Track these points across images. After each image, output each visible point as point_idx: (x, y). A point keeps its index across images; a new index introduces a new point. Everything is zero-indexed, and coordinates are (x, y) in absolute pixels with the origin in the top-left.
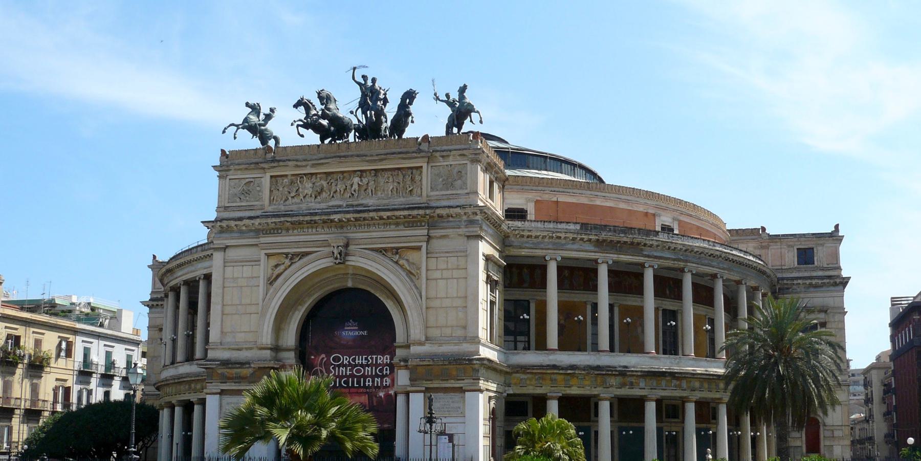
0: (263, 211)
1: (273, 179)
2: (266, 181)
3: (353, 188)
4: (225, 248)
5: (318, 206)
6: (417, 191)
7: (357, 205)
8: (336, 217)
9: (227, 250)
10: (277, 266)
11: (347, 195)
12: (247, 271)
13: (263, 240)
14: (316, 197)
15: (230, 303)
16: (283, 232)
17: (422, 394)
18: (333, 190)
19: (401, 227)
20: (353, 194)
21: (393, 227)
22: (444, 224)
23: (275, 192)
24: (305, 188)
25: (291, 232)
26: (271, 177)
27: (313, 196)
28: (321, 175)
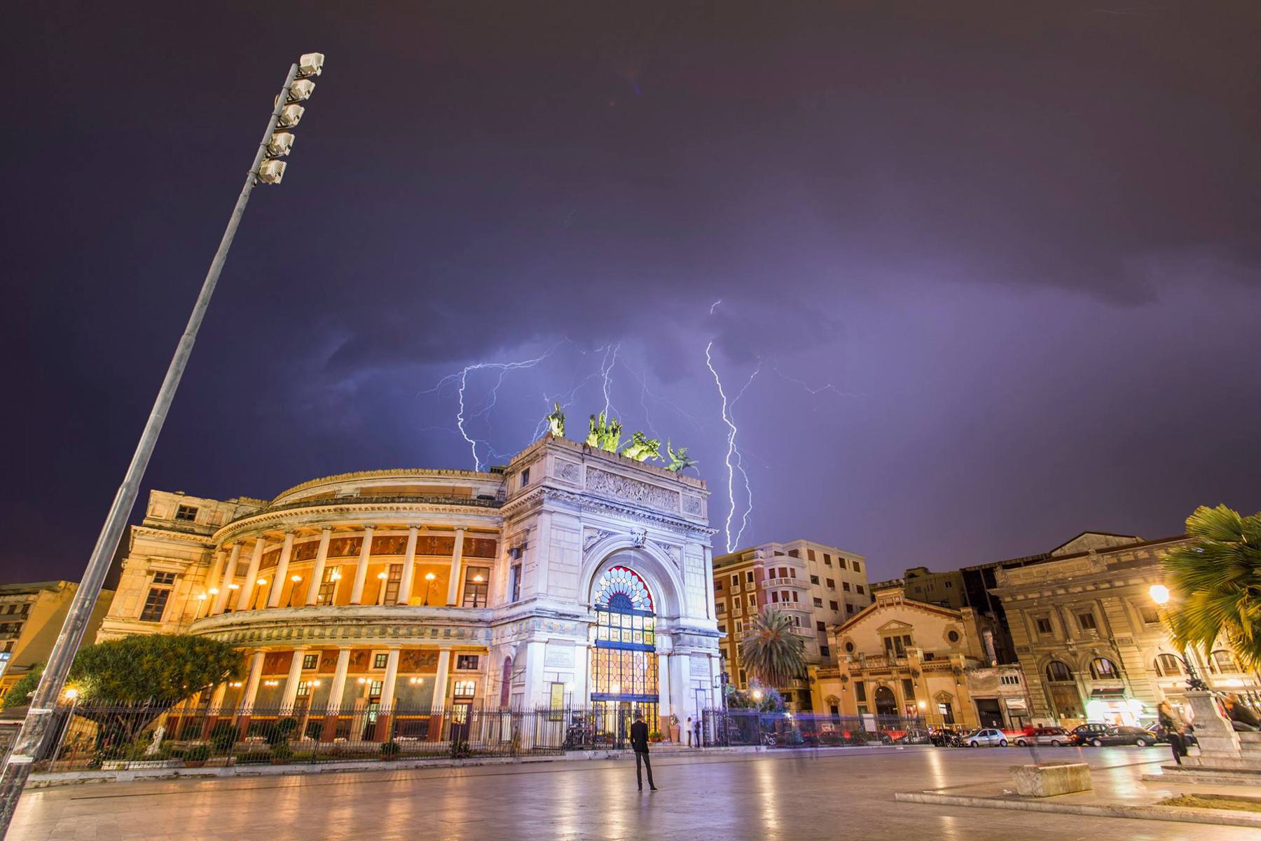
1: (589, 470)
2: (583, 468)
4: (553, 512)
6: (675, 508)
9: (553, 514)
10: (589, 538)
12: (568, 536)
13: (583, 514)
14: (616, 492)
15: (554, 561)
17: (688, 657)
19: (671, 530)
20: (640, 499)
21: (667, 529)
22: (693, 536)
23: (589, 479)
25: (603, 514)
27: (615, 491)
28: (620, 478)
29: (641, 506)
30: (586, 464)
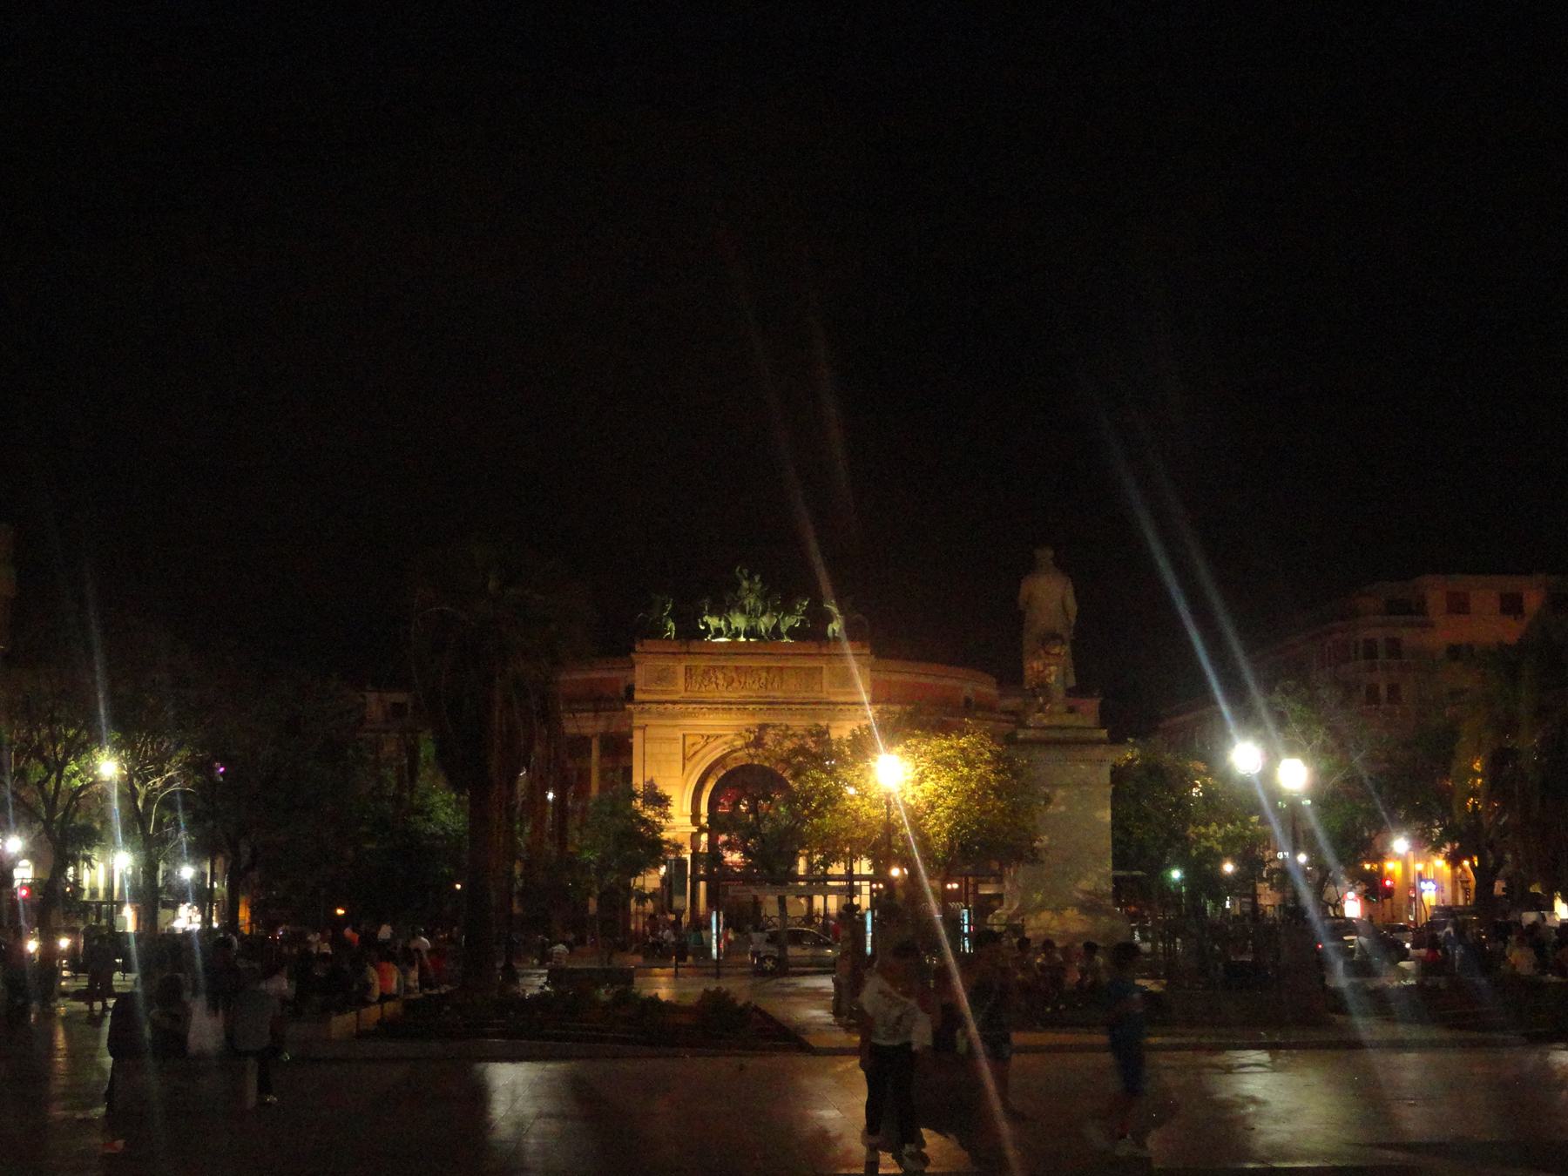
0: (680, 695)
2: (681, 669)
3: (762, 681)
5: (732, 695)
7: (766, 697)
8: (751, 707)
11: (756, 686)
14: (727, 688)
16: (701, 716)
18: (742, 680)
19: (806, 717)
21: (798, 717)
24: (717, 678)
25: (707, 716)
26: (686, 666)
27: (725, 685)
29: (760, 697)
30: (684, 664)
